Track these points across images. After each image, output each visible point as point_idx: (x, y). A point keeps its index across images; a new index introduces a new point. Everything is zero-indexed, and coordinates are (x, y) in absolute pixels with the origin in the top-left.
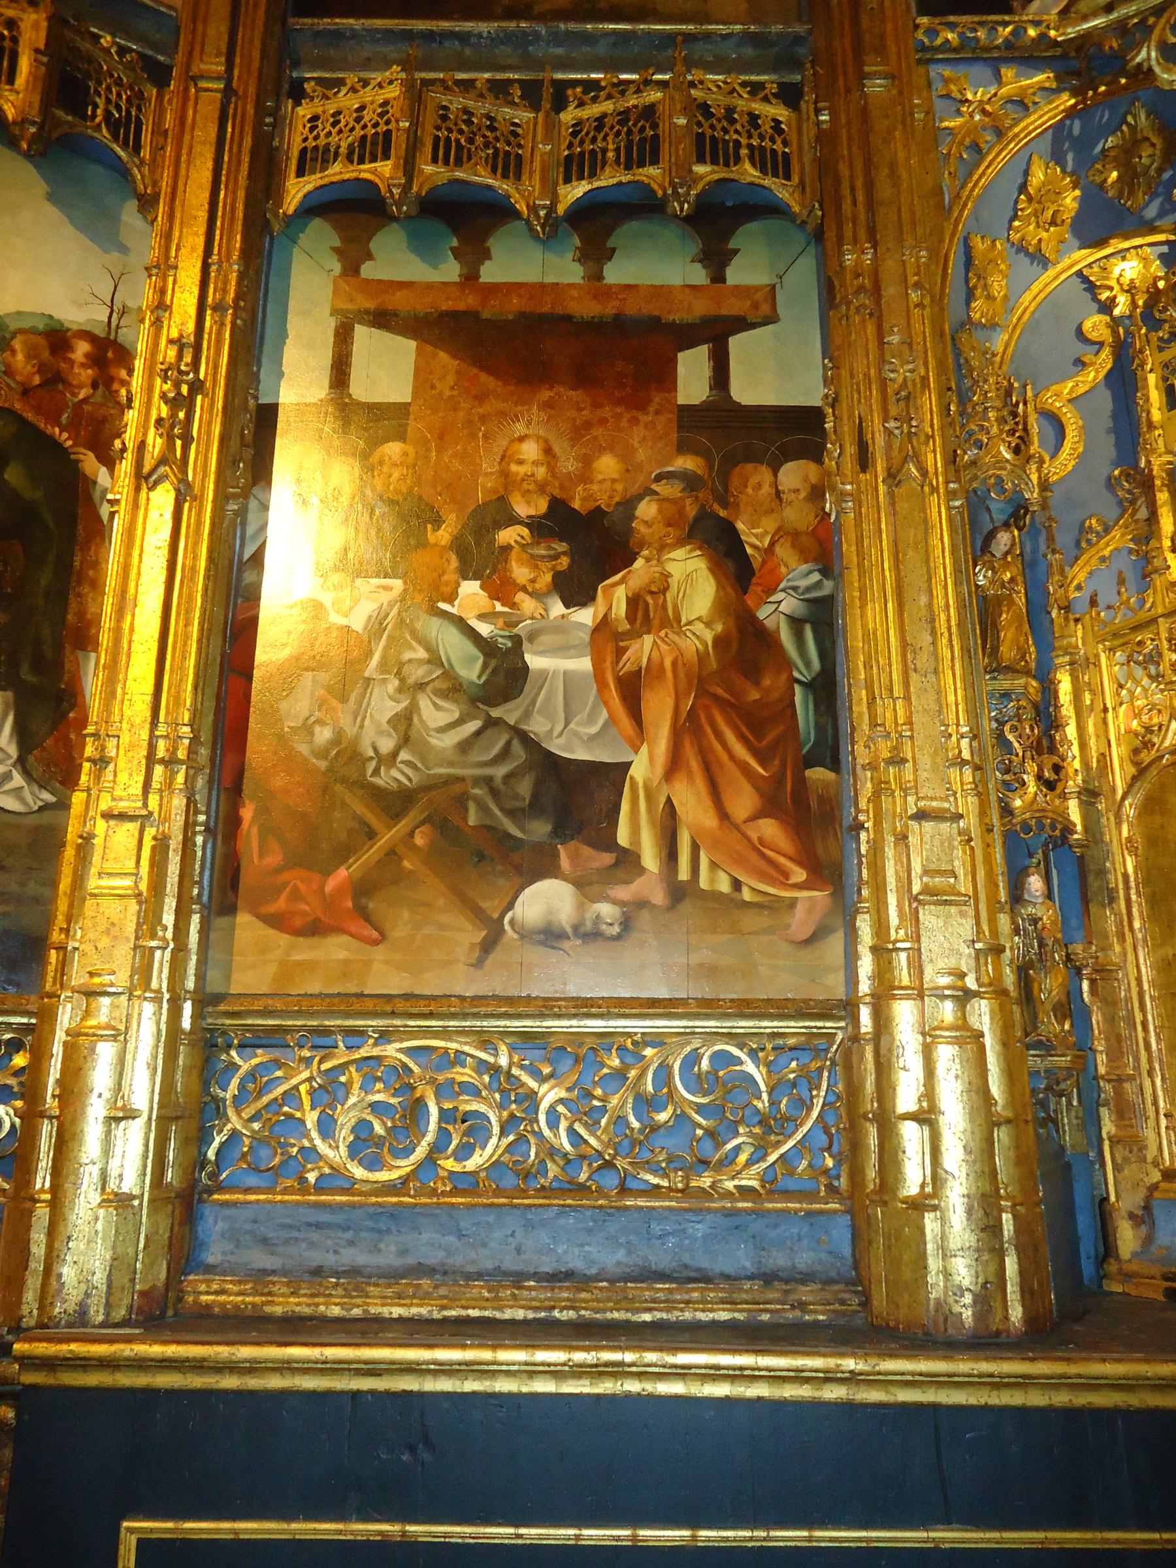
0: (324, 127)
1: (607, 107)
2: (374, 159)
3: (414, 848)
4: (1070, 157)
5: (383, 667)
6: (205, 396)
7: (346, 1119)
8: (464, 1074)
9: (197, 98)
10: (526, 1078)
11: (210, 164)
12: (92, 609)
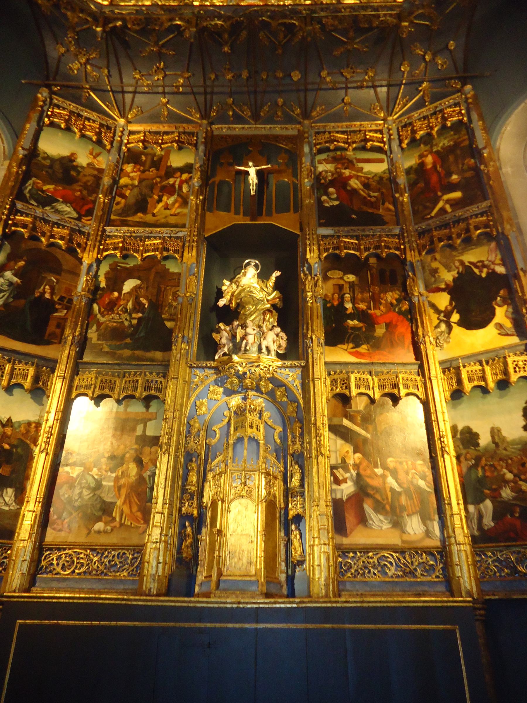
0: (81, 381)
1: (131, 379)
8: (82, 556)
10: (91, 556)
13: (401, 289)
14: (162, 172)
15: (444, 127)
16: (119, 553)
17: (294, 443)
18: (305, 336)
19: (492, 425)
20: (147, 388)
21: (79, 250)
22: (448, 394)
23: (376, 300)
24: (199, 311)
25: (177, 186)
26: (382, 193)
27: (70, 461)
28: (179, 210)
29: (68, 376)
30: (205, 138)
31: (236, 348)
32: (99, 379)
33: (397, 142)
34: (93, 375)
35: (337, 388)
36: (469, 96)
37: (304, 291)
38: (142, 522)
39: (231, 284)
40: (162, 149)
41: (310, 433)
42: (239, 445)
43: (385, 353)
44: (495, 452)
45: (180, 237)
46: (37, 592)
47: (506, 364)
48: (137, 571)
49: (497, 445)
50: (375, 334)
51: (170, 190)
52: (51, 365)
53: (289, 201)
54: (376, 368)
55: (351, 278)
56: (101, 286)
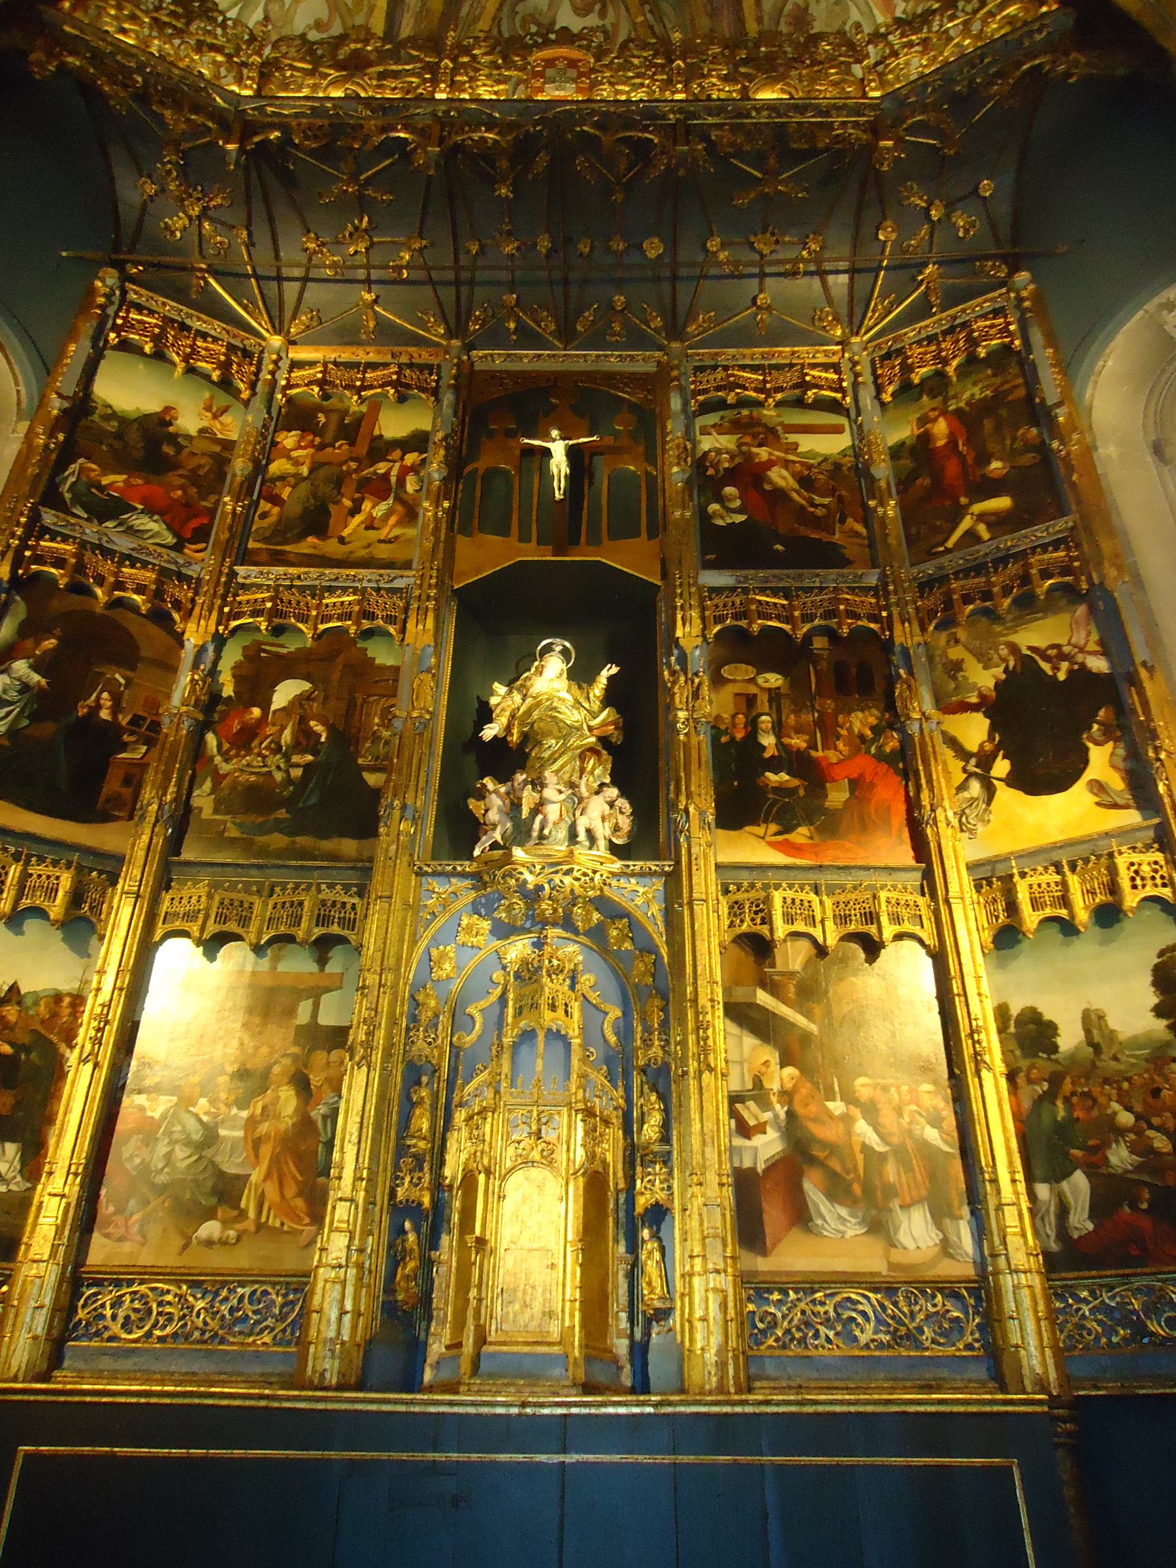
5: (164, 1134)
7: (121, 1313)
8: (169, 1298)
10: (191, 1299)
13: (882, 705)
14: (362, 449)
15: (972, 360)
16: (254, 1292)
17: (647, 1044)
18: (672, 806)
19: (1085, 1006)
20: (322, 920)
21: (176, 616)
22: (988, 936)
23: (827, 729)
24: (439, 750)
25: (393, 479)
26: (840, 499)
27: (148, 1083)
28: (397, 532)
29: (146, 891)
30: (456, 378)
31: (521, 833)
32: (217, 898)
33: (872, 388)
34: (202, 890)
35: (742, 921)
36: (1025, 294)
37: (670, 707)
38: (307, 1220)
39: (510, 692)
40: (362, 400)
41: (682, 1020)
42: (524, 1049)
43: (848, 845)
44: (1093, 1063)
45: (400, 590)
46: (64, 1380)
47: (1113, 871)
48: (293, 1333)
49: (1097, 1048)
50: (827, 804)
51: (380, 488)
52: (110, 867)
53: (637, 513)
54: (829, 877)
55: (774, 680)
56: (224, 695)
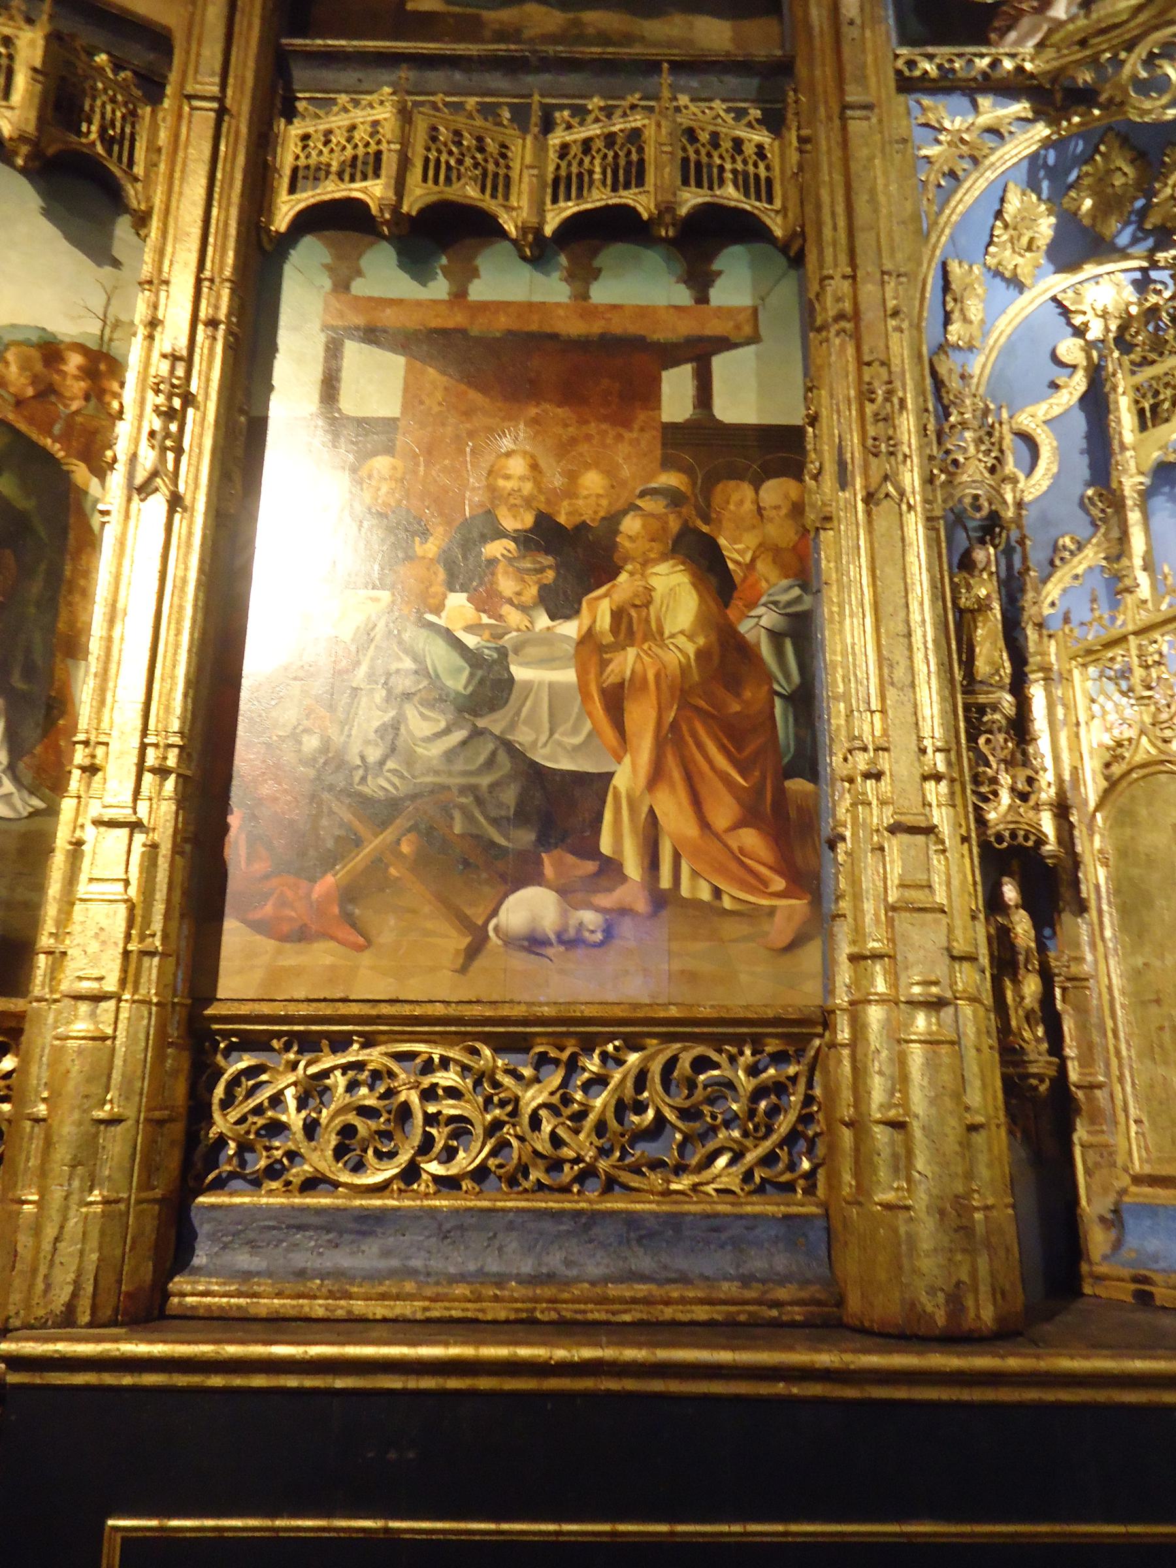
0: (317, 143)
1: (594, 130)
2: (365, 178)
3: (400, 855)
4: (1045, 185)
5: (371, 677)
6: (197, 408)
8: (447, 1078)
9: (190, 115)
10: (507, 1081)
11: (204, 181)
12: (84, 618)
16: (670, 1065)
20: (693, 172)
38: (779, 884)
